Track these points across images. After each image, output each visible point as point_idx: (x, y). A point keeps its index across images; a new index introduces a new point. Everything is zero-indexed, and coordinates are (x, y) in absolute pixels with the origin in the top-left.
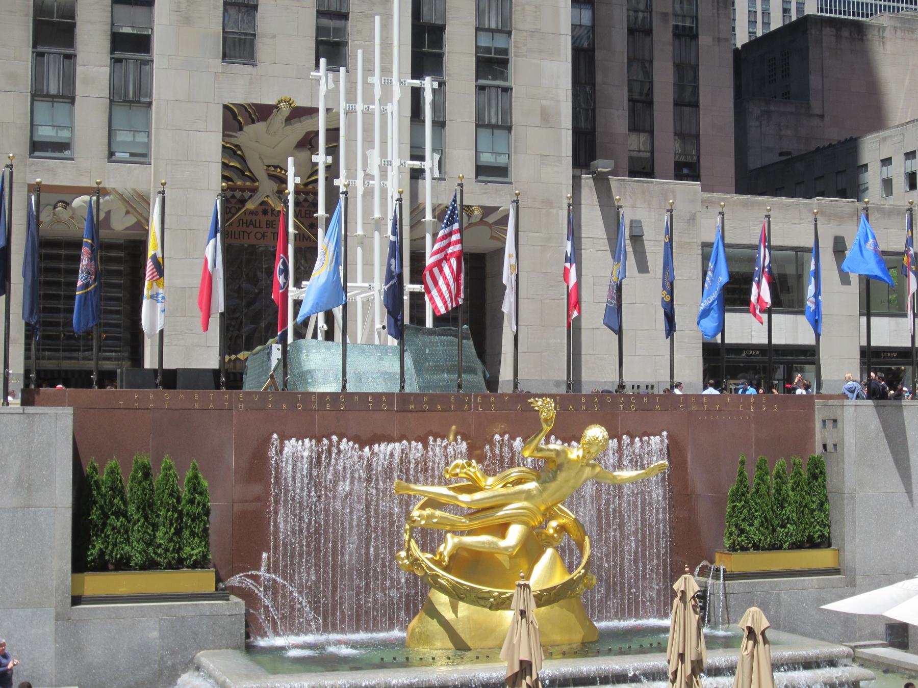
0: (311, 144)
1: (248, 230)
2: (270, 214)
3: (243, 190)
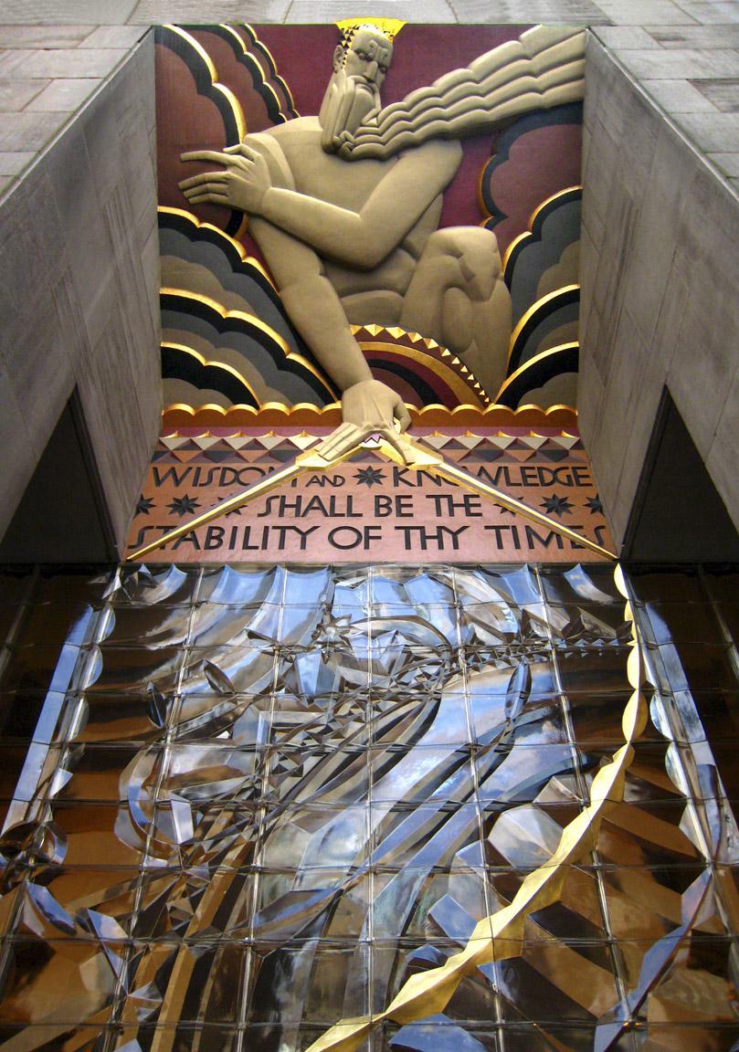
1: (304, 525)
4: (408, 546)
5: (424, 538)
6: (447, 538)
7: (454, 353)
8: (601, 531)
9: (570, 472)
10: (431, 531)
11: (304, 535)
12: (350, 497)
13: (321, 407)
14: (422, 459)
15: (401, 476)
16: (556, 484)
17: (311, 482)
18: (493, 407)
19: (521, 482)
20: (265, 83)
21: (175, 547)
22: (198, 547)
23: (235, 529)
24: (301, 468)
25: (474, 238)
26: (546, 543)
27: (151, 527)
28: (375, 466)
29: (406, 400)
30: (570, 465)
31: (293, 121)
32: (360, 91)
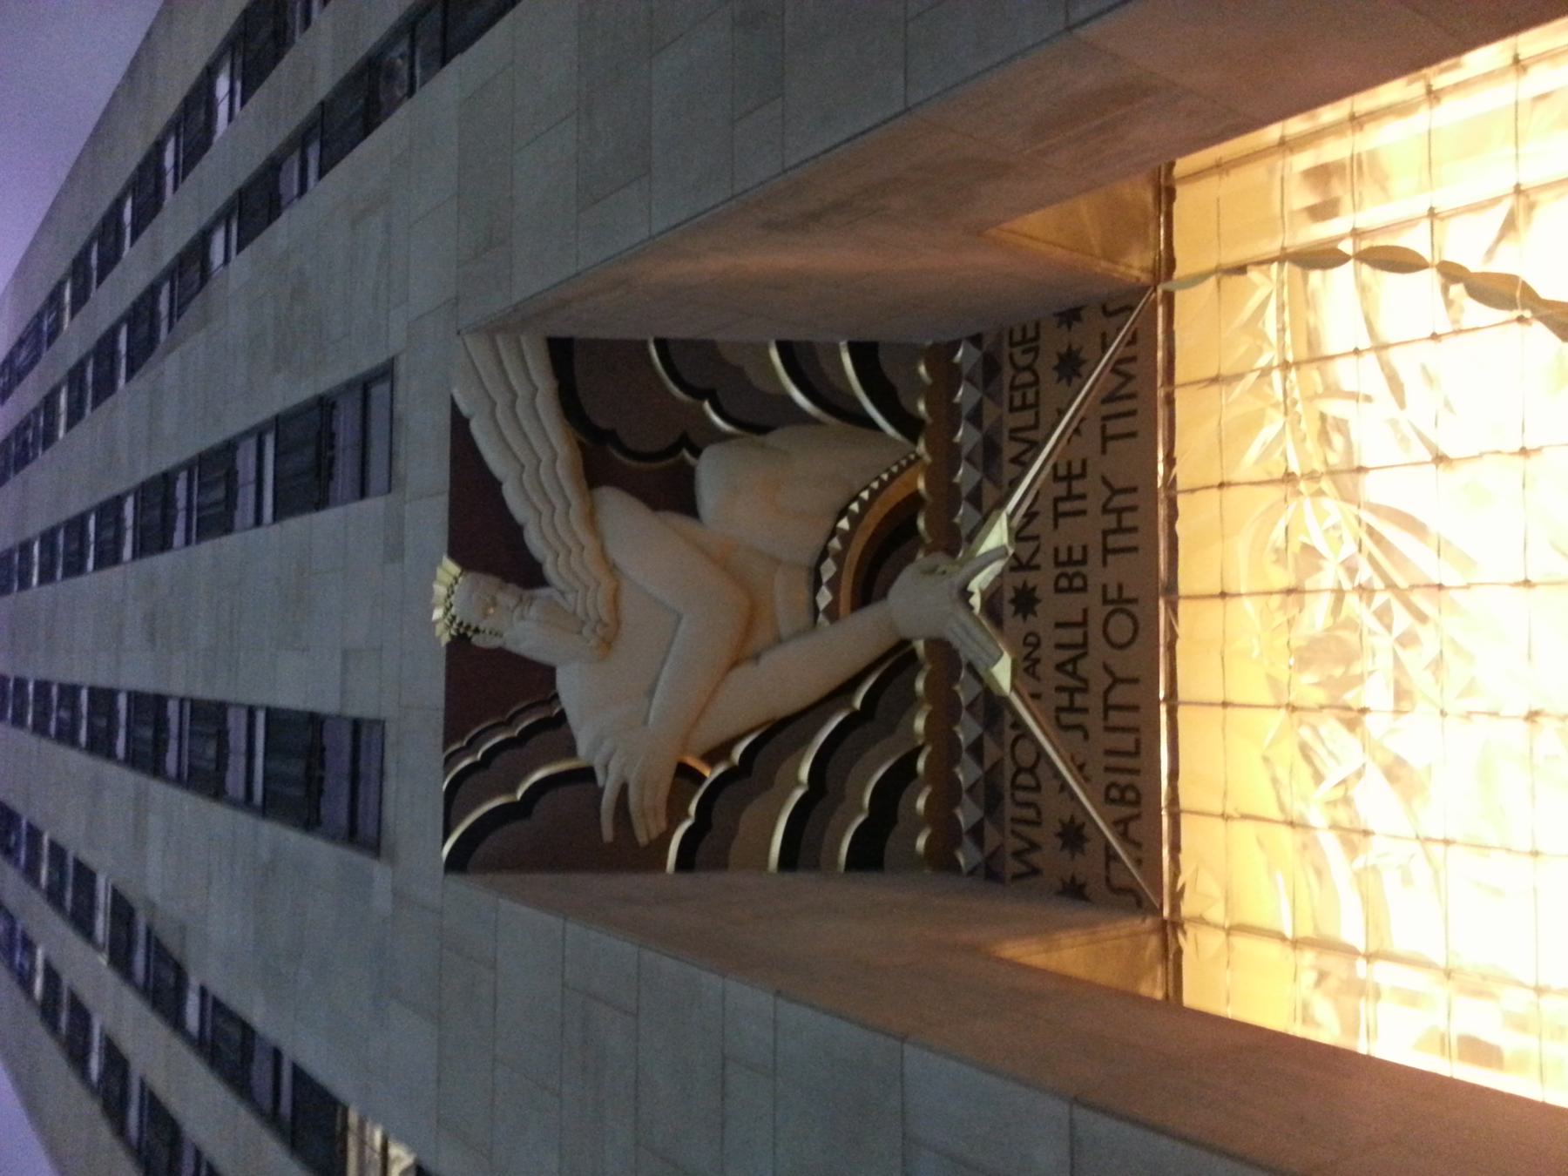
0: (673, 450)
1: (1099, 682)
2: (1032, 578)
3: (946, 712)
4: (1134, 549)
5: (1120, 530)
6: (1120, 501)
7: (856, 498)
8: (1111, 308)
9: (1017, 351)
10: (1110, 521)
11: (1117, 680)
12: (1059, 625)
13: (920, 667)
14: (997, 536)
15: (1024, 560)
16: (1036, 366)
17: (1034, 675)
18: (921, 447)
19: (1032, 412)
20: (516, 733)
21: (1138, 845)
22: (1138, 816)
23: (1108, 769)
24: (1014, 687)
25: (713, 474)
26: (1129, 378)
27: (1108, 880)
28: (1009, 594)
29: (911, 559)
30: (1006, 349)
31: (563, 697)
32: (533, 612)
